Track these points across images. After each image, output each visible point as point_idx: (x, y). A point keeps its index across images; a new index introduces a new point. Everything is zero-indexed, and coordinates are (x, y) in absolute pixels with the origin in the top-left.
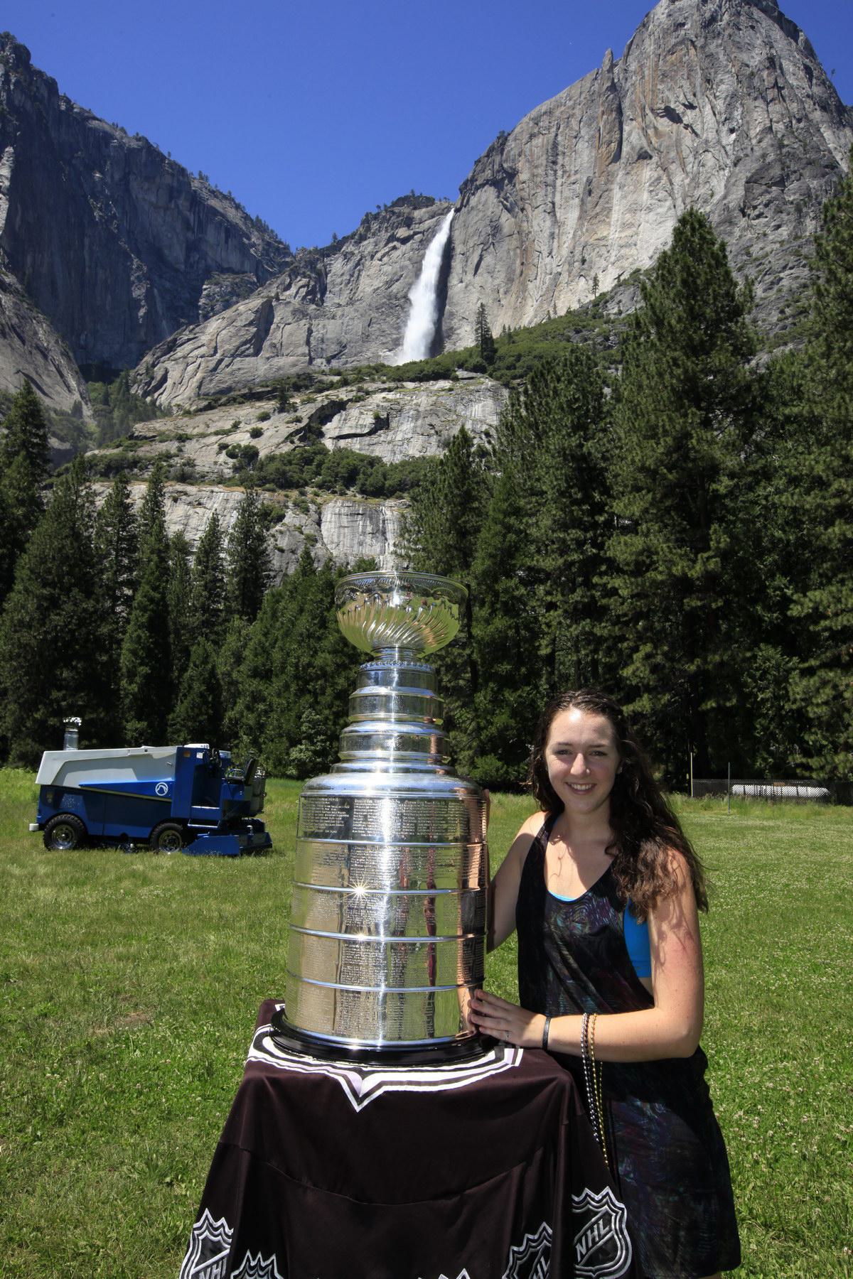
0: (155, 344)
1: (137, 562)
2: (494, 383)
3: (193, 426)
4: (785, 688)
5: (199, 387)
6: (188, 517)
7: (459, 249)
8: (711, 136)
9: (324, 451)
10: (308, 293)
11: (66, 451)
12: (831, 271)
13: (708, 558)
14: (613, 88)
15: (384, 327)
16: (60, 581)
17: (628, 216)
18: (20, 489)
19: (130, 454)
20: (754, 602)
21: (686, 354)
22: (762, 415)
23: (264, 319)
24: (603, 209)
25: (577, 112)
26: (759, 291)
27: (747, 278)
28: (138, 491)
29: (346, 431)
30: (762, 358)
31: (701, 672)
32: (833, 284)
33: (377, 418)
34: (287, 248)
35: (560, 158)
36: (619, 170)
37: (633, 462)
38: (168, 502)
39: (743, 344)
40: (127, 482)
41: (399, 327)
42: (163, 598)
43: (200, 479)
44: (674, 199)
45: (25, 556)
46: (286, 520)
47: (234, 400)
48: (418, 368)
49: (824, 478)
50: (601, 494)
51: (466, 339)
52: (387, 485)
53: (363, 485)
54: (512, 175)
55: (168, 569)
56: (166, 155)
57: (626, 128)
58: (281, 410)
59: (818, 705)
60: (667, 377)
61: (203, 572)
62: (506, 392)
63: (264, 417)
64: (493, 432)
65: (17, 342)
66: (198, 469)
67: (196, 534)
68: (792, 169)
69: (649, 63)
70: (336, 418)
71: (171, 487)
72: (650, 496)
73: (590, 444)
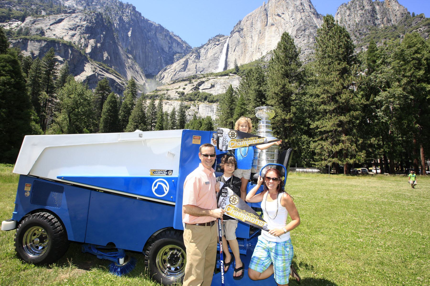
0: (162, 69)
1: (156, 118)
3: (169, 87)
4: (309, 146)
5: (172, 79)
6: (169, 108)
9: (199, 93)
10: (196, 57)
12: (320, 45)
15: (213, 64)
16: (139, 122)
19: (156, 94)
20: (301, 125)
21: (285, 65)
22: (303, 80)
23: (186, 63)
28: (157, 102)
31: (289, 142)
32: (320, 48)
33: (212, 85)
34: (191, 47)
37: (272, 92)
39: (298, 63)
40: (155, 100)
42: (162, 126)
45: (131, 116)
47: (179, 81)
49: (319, 94)
50: (264, 100)
52: (214, 100)
55: (163, 119)
56: (164, 27)
58: (190, 83)
59: (317, 149)
60: (280, 71)
61: (171, 120)
63: (186, 85)
67: (169, 112)
70: (202, 85)
72: (276, 99)
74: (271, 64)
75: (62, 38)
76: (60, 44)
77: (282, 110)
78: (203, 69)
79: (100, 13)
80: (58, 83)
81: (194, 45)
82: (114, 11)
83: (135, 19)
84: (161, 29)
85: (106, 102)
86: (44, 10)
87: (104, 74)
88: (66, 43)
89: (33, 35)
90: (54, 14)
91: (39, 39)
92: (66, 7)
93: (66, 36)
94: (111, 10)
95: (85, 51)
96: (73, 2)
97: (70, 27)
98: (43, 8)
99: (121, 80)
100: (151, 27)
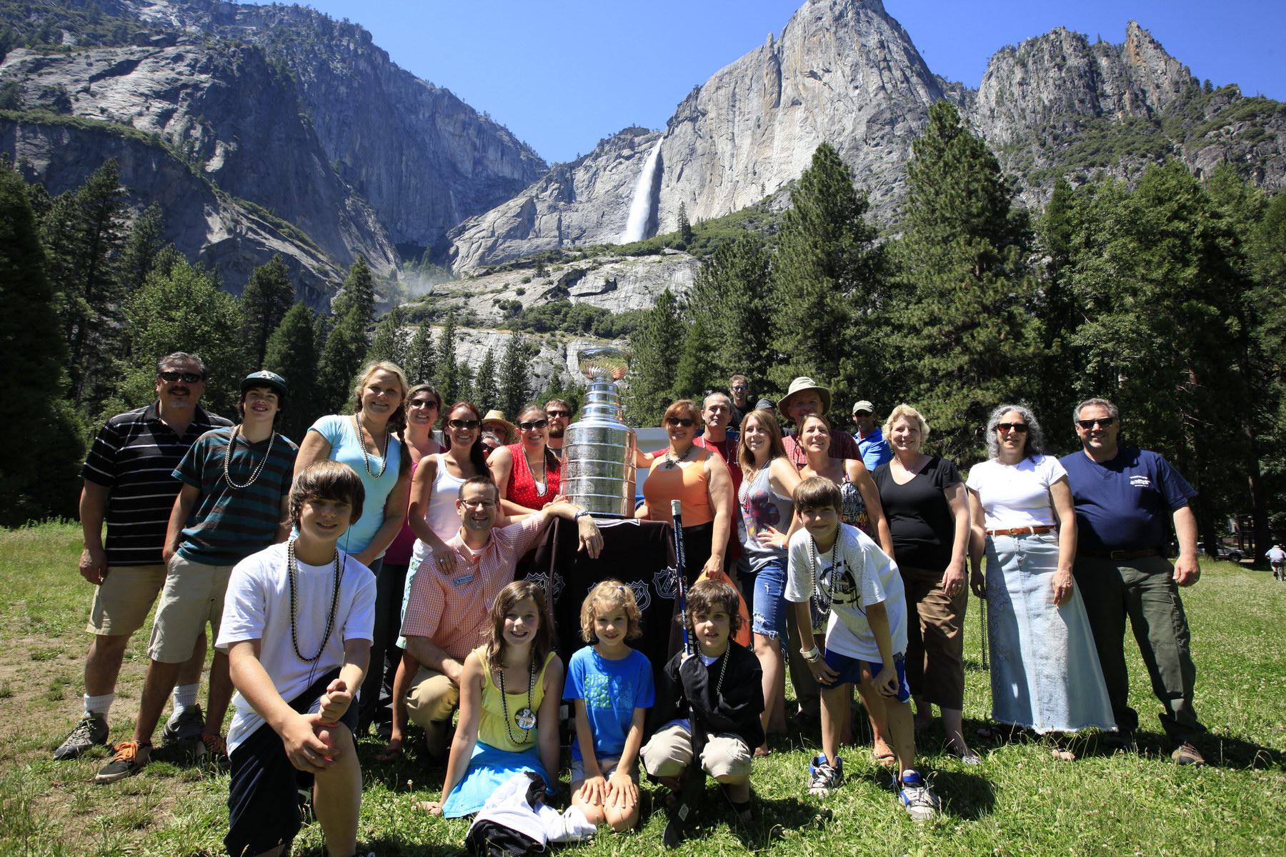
2: (691, 257)
3: (475, 287)
5: (482, 258)
6: (470, 351)
7: (666, 164)
8: (842, 91)
9: (569, 305)
11: (385, 305)
13: (838, 382)
14: (776, 59)
15: (612, 218)
17: (786, 143)
18: (353, 330)
19: (430, 307)
23: (528, 213)
24: (768, 138)
25: (749, 73)
26: (875, 198)
27: (869, 186)
28: (437, 332)
29: (584, 291)
30: (876, 243)
34: (544, 162)
35: (737, 103)
36: (780, 113)
37: (787, 313)
38: (457, 340)
40: (428, 326)
41: (625, 217)
43: (482, 324)
44: (818, 132)
46: (541, 355)
47: (505, 268)
48: (637, 247)
51: (670, 226)
52: (614, 328)
53: (597, 329)
54: (704, 115)
55: (457, 387)
57: (783, 84)
58: (539, 275)
61: (482, 391)
62: (699, 264)
63: (527, 281)
64: (690, 293)
65: (354, 229)
66: (479, 317)
67: (476, 365)
68: (899, 113)
69: (799, 42)
71: (460, 330)
73: (756, 301)
74: (786, 232)
75: (130, 123)
76: (121, 139)
77: (817, 369)
78: (579, 232)
79: (255, 48)
80: (124, 270)
81: (553, 154)
82: (300, 44)
83: (369, 70)
84: (449, 103)
85: (278, 333)
86: (70, 29)
87: (264, 241)
88: (140, 136)
89: (30, 108)
90: (105, 44)
91: (51, 121)
92: (145, 22)
93: (140, 114)
94: (292, 40)
95: (205, 166)
96: (170, 10)
97: (157, 87)
98: (69, 23)
99: (318, 260)
100: (419, 98)
